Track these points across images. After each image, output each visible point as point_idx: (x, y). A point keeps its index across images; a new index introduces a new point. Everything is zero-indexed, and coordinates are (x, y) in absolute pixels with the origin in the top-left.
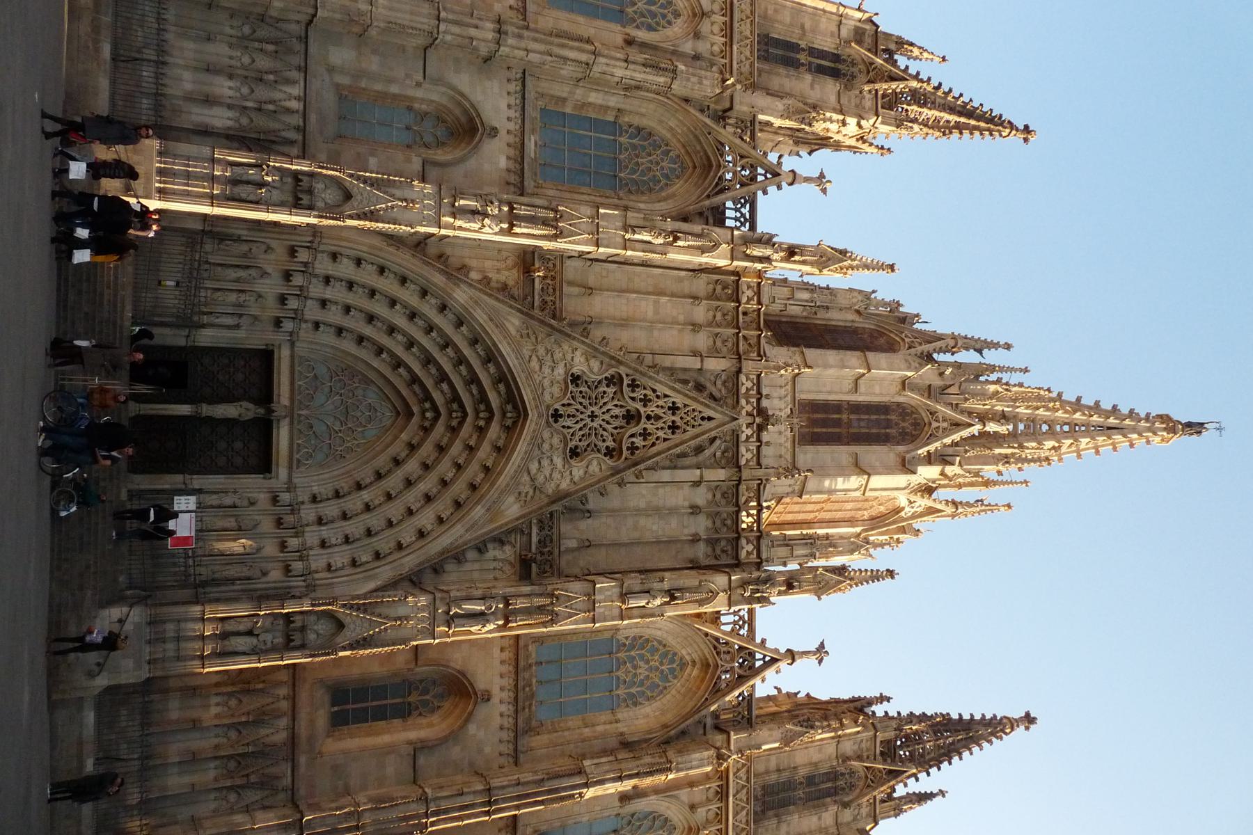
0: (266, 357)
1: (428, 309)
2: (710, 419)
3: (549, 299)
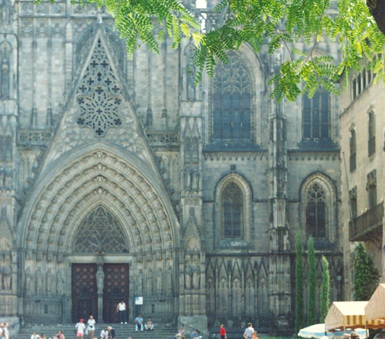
0: (74, 266)
1: (50, 195)
2: (99, 41)
3: (41, 137)
